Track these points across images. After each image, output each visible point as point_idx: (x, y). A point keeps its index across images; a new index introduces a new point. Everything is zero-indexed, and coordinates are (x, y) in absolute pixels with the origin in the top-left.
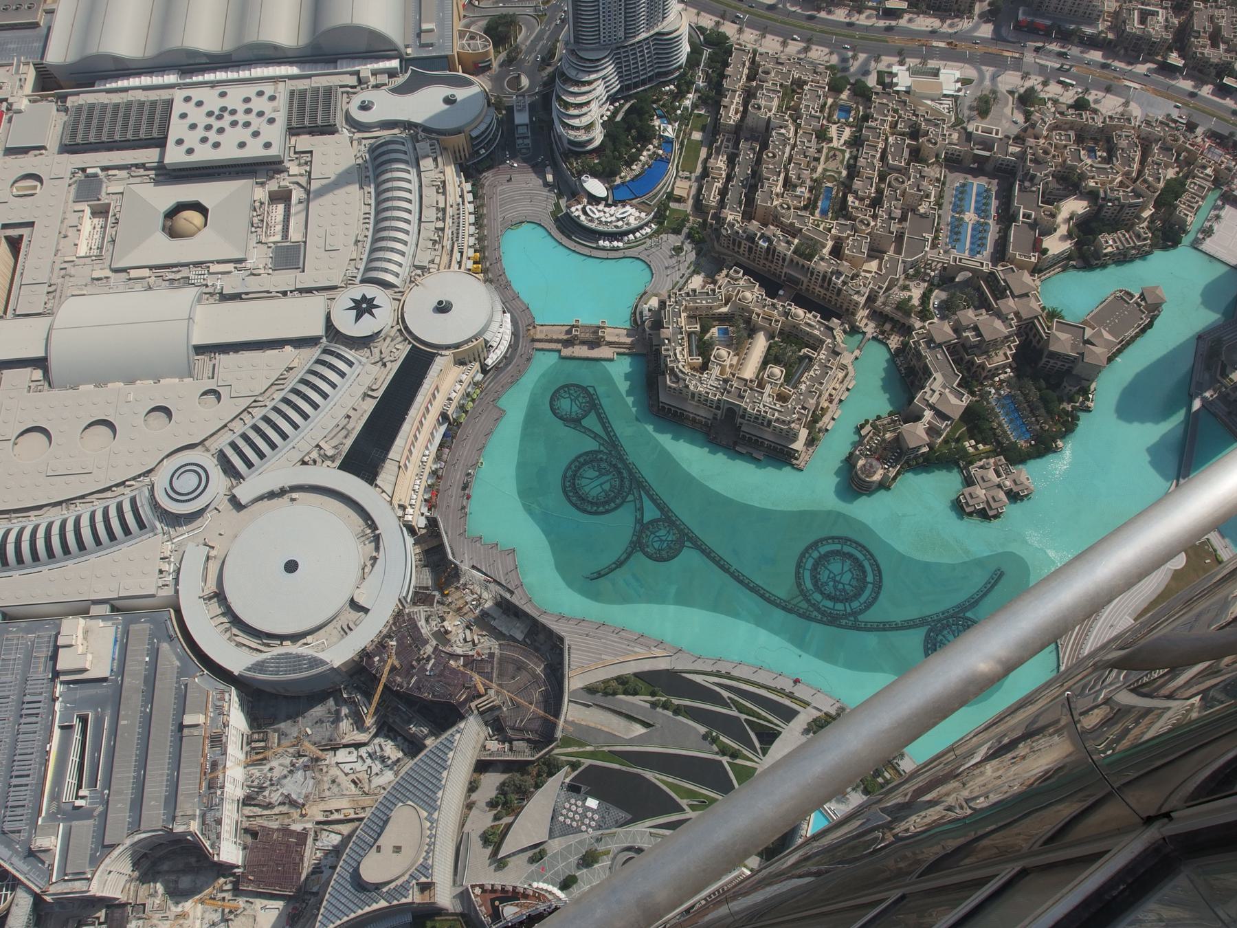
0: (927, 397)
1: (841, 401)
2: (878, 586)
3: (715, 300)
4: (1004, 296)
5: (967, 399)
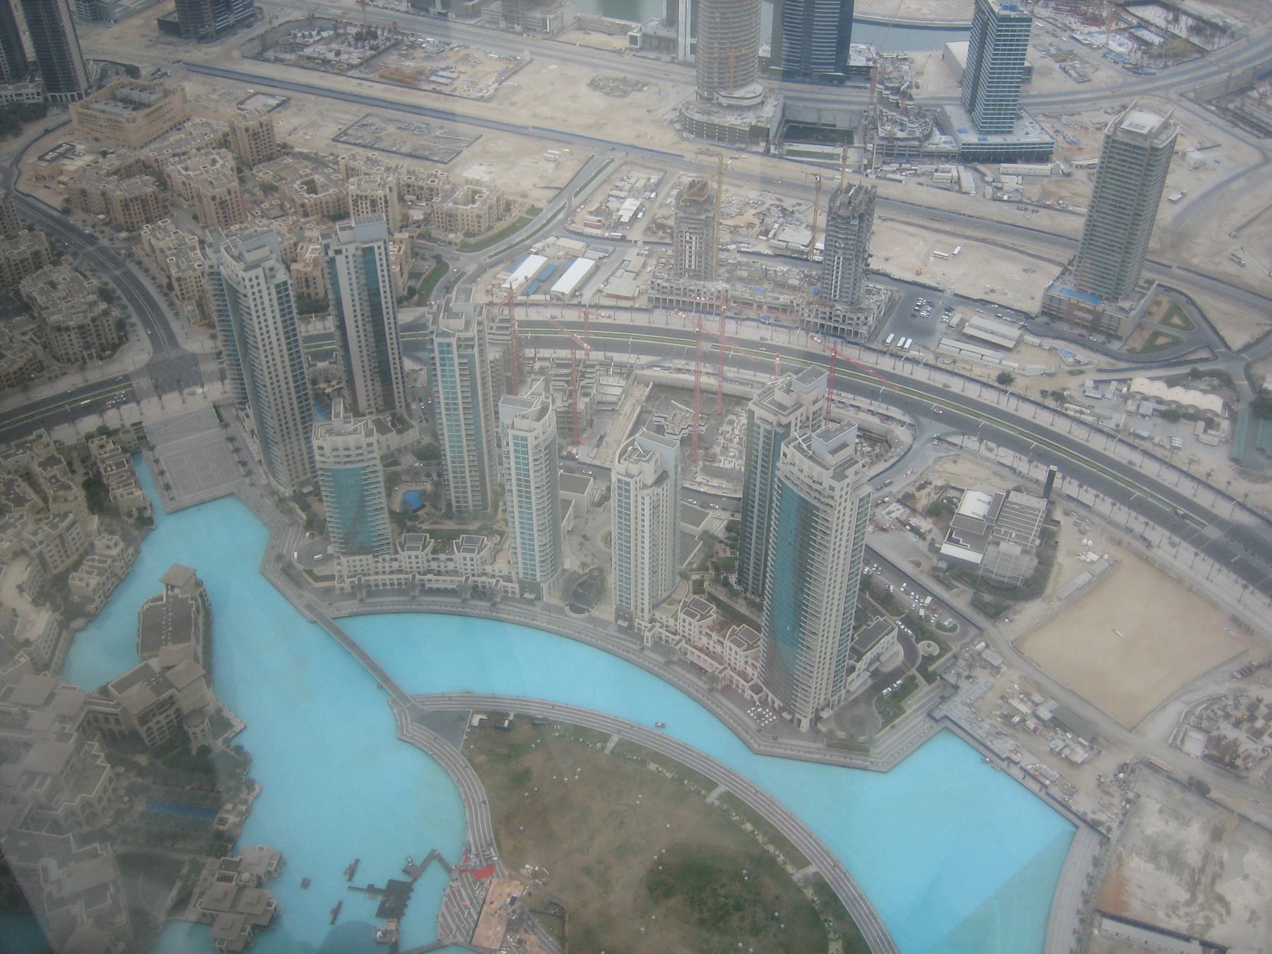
4: (26, 716)
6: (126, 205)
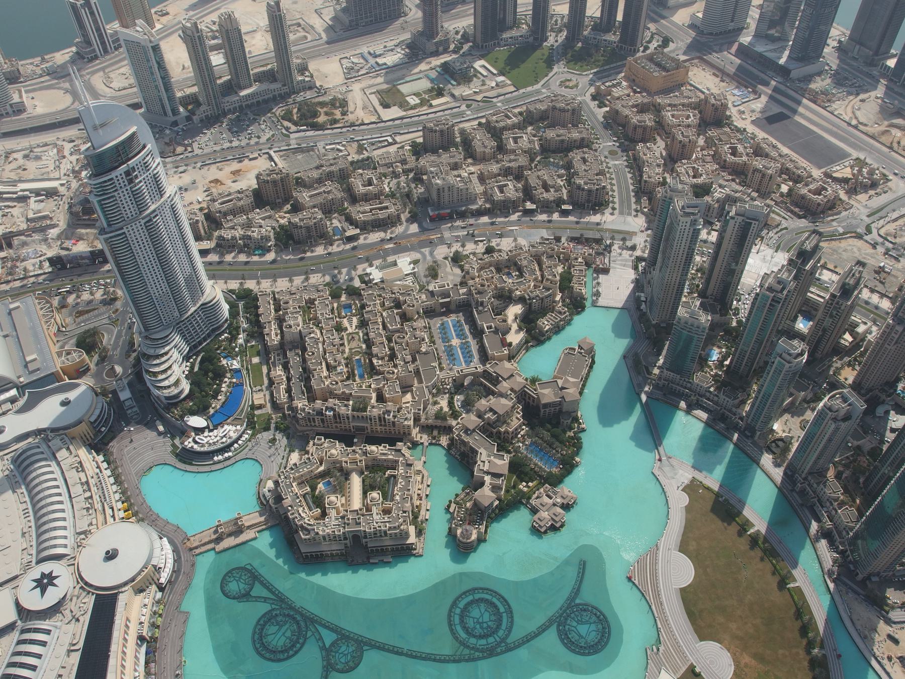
0: (481, 468)
1: (427, 496)
2: (510, 611)
3: (312, 465)
4: (498, 382)
5: (507, 458)
6: (635, 127)
